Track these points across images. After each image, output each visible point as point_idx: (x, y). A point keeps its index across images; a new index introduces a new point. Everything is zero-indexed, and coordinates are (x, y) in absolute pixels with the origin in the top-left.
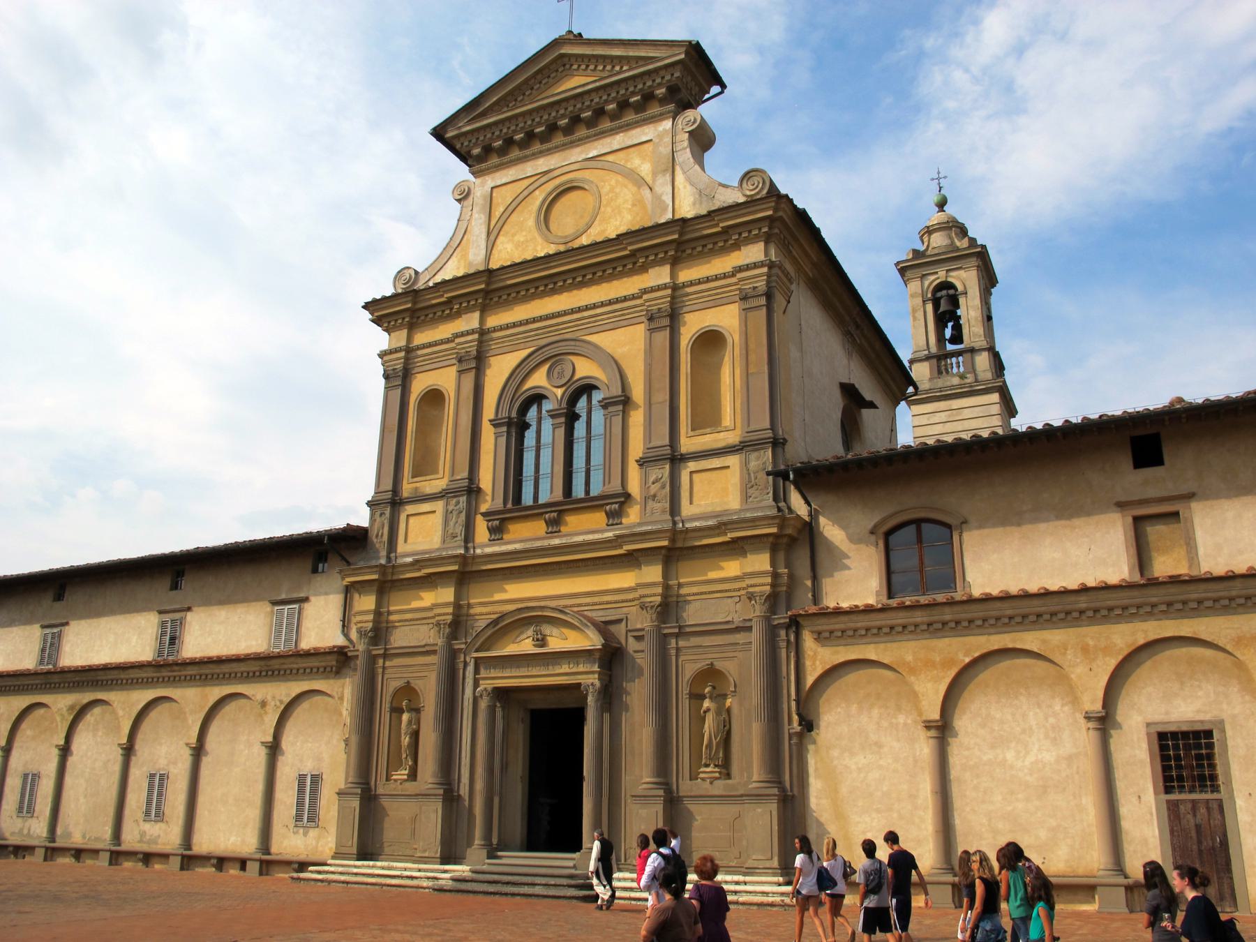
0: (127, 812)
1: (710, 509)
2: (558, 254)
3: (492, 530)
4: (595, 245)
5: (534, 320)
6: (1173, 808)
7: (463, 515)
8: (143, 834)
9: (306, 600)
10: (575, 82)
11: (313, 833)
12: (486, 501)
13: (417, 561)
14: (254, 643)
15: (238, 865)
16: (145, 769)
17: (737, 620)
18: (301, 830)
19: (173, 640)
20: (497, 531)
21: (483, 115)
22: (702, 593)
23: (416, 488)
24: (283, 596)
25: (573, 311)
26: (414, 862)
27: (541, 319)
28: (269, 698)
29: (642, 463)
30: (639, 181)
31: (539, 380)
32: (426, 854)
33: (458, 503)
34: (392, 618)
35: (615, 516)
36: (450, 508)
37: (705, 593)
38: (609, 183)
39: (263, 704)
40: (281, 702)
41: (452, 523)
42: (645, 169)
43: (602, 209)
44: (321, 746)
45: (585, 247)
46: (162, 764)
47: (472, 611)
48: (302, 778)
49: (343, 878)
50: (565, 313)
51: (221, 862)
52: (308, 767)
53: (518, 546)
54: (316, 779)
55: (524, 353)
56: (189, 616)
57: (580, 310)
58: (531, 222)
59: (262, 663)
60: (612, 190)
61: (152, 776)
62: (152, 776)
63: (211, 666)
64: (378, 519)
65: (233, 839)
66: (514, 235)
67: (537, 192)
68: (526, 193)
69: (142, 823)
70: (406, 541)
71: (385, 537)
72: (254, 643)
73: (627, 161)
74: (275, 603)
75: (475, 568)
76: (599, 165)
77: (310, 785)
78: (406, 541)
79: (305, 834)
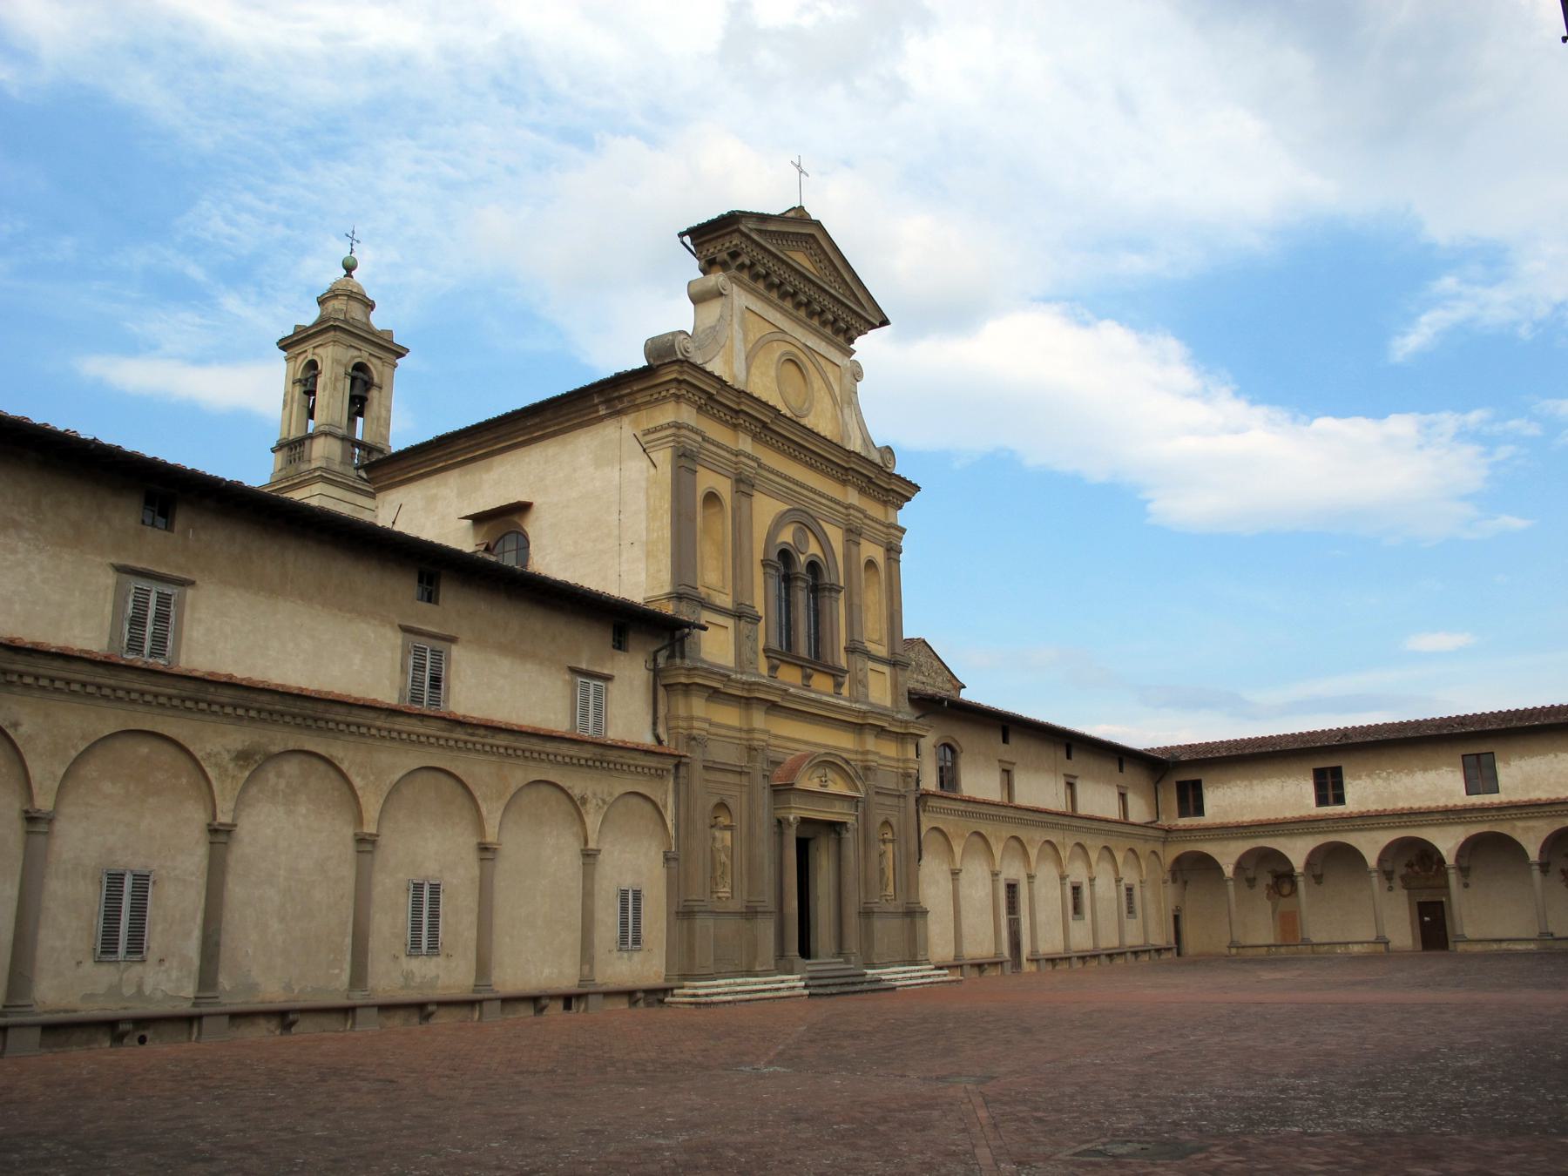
0: (374, 943)
6: (1010, 920)
8: (408, 976)
9: (608, 678)
10: (801, 259)
11: (637, 957)
14: (552, 716)
15: (560, 1004)
16: (401, 875)
18: (625, 955)
19: (436, 681)
21: (760, 232)
24: (584, 666)
28: (589, 794)
31: (787, 536)
35: (838, 685)
39: (584, 800)
40: (604, 802)
44: (635, 862)
46: (430, 870)
48: (624, 893)
49: (729, 998)
51: (536, 1001)
52: (628, 882)
54: (637, 895)
55: (787, 507)
56: (456, 651)
59: (598, 751)
61: (418, 887)
62: (418, 887)
63: (534, 740)
65: (547, 971)
69: (403, 959)
72: (552, 716)
74: (575, 671)
77: (631, 901)
79: (630, 959)
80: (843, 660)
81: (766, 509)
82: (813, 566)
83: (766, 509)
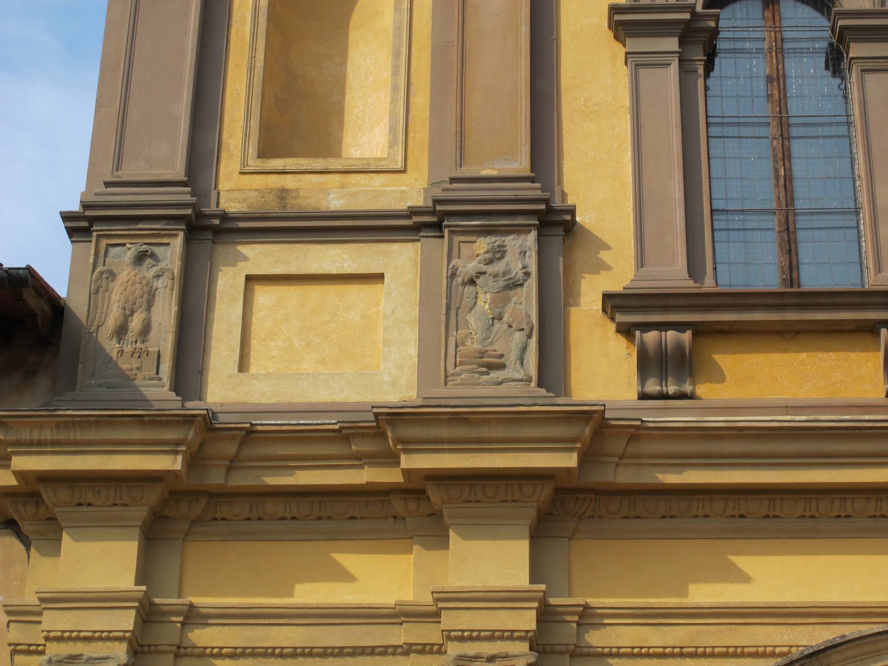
3: (649, 364)
7: (526, 302)
12: (601, 267)
23: (283, 194)
33: (499, 253)
34: (201, 637)
36: (470, 267)
41: (474, 321)
47: (596, 638)
64: (126, 273)
70: (243, 365)
71: (164, 339)
75: (626, 477)
78: (243, 365)
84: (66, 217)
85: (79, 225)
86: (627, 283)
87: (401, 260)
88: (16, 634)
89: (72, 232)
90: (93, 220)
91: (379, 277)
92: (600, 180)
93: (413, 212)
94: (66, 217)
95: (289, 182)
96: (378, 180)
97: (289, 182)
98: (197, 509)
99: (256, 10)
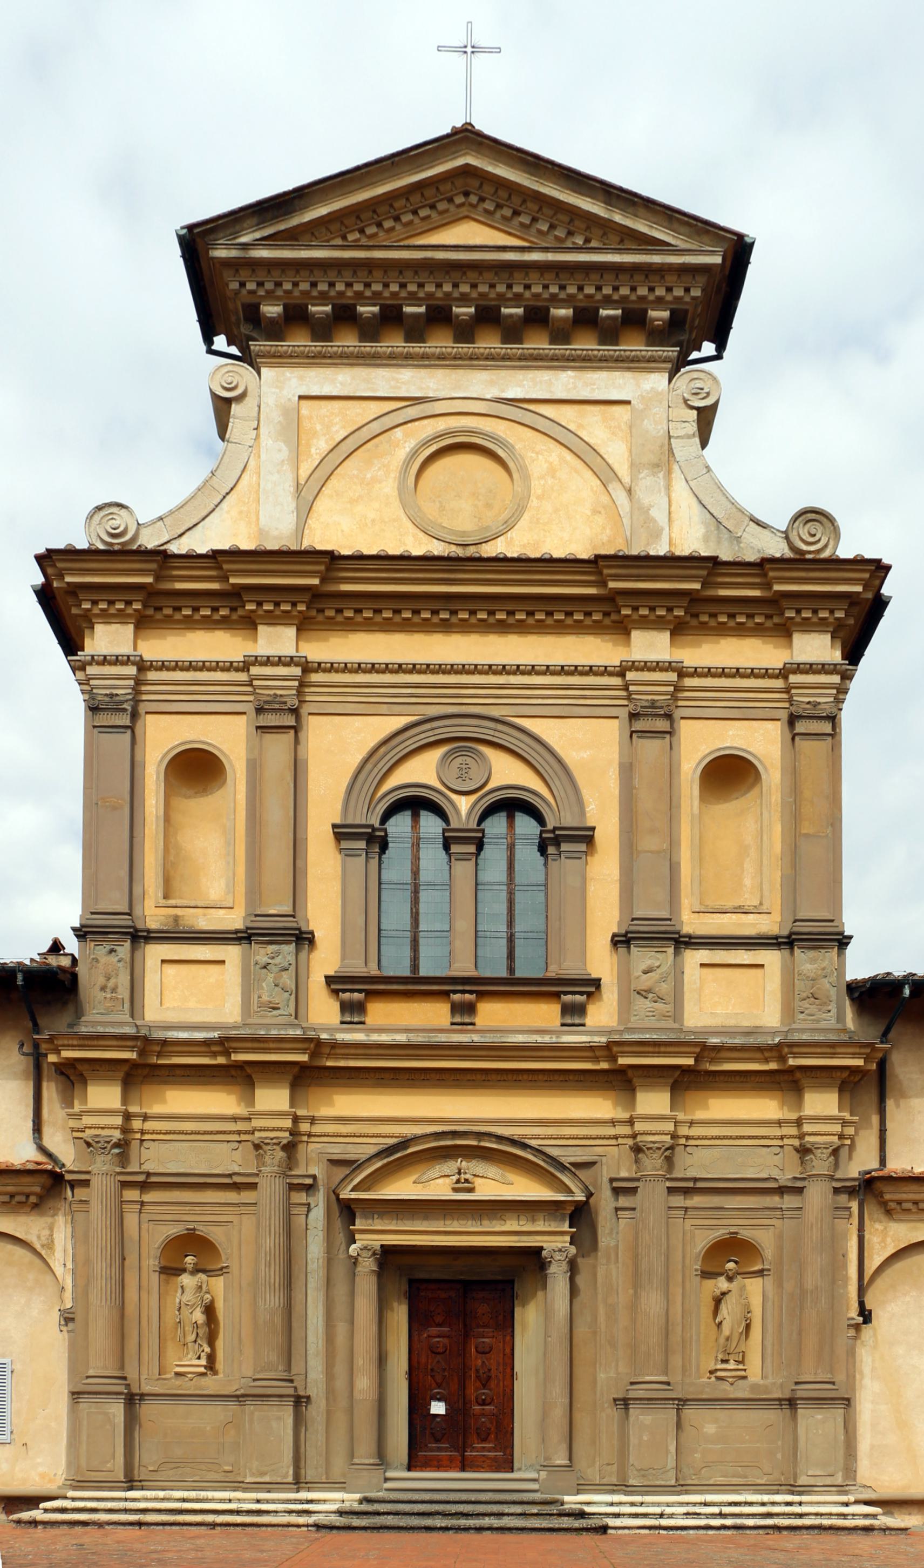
1: (732, 1022)
2: (448, 559)
3: (346, 1007)
4: (523, 562)
5: (414, 669)
13: (222, 1041)
17: (785, 1178)
20: (353, 1011)
22: (725, 1138)
23: (176, 919)
25: (490, 669)
26: (245, 1490)
27: (428, 669)
29: (622, 941)
30: (604, 474)
31: (422, 771)
32: (267, 1479)
35: (574, 1012)
37: (731, 1138)
38: (539, 456)
42: (617, 453)
43: (534, 502)
45: (506, 559)
50: (476, 670)
53: (401, 1038)
57: (504, 670)
58: (389, 487)
60: (552, 472)
66: (353, 501)
67: (398, 432)
68: (376, 427)
73: (580, 426)
76: (528, 418)
80: (600, 962)
81: (338, 745)
82: (512, 805)
83: (338, 745)
84: (74, 929)
85: (81, 933)
86: (336, 968)
87: (232, 953)
88: (73, 1123)
89: (77, 936)
90: (87, 933)
91: (223, 962)
92: (324, 914)
93: (237, 932)
94: (74, 929)
95: (178, 912)
96: (222, 912)
97: (178, 912)
98: (146, 1071)
99: (157, 817)
